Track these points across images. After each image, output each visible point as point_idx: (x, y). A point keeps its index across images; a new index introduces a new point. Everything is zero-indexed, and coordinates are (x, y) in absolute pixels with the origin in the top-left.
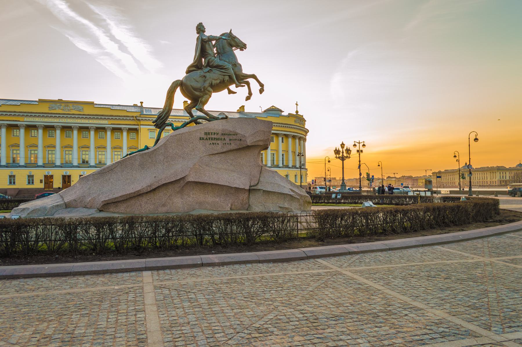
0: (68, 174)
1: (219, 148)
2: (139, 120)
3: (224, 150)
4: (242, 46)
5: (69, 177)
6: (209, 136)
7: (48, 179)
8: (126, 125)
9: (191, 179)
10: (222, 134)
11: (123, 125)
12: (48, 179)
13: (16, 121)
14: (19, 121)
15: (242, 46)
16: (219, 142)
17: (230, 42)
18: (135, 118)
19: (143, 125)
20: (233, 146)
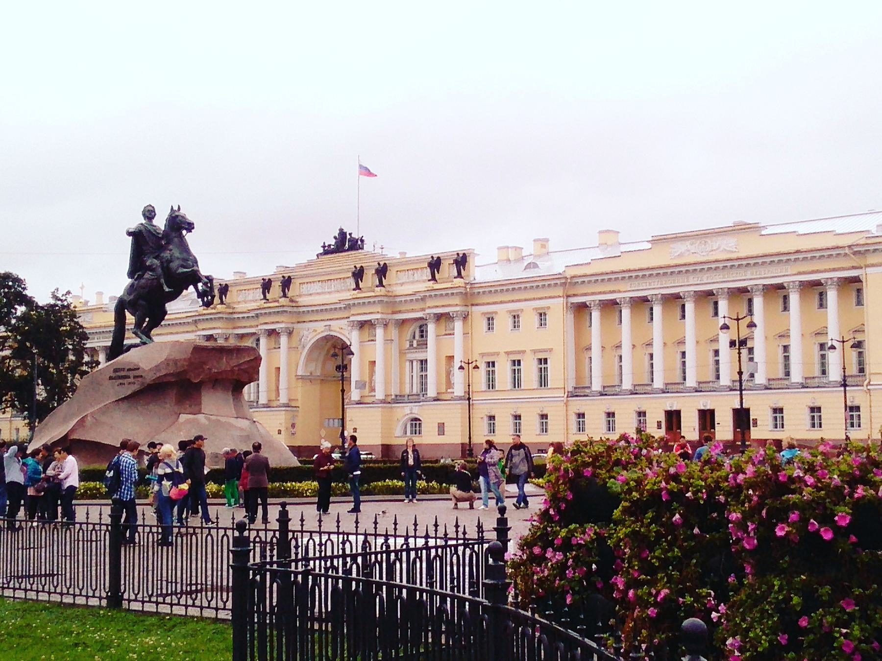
0: (709, 407)
1: (128, 390)
2: (859, 252)
3: (129, 392)
4: (190, 227)
5: (712, 412)
6: (118, 374)
7: (673, 418)
8: (834, 270)
9: (75, 436)
10: (129, 370)
11: (825, 271)
12: (673, 418)
13: (614, 292)
14: (619, 292)
15: (190, 227)
16: (125, 381)
17: (178, 225)
18: (847, 251)
19: (873, 265)
20: (136, 387)
